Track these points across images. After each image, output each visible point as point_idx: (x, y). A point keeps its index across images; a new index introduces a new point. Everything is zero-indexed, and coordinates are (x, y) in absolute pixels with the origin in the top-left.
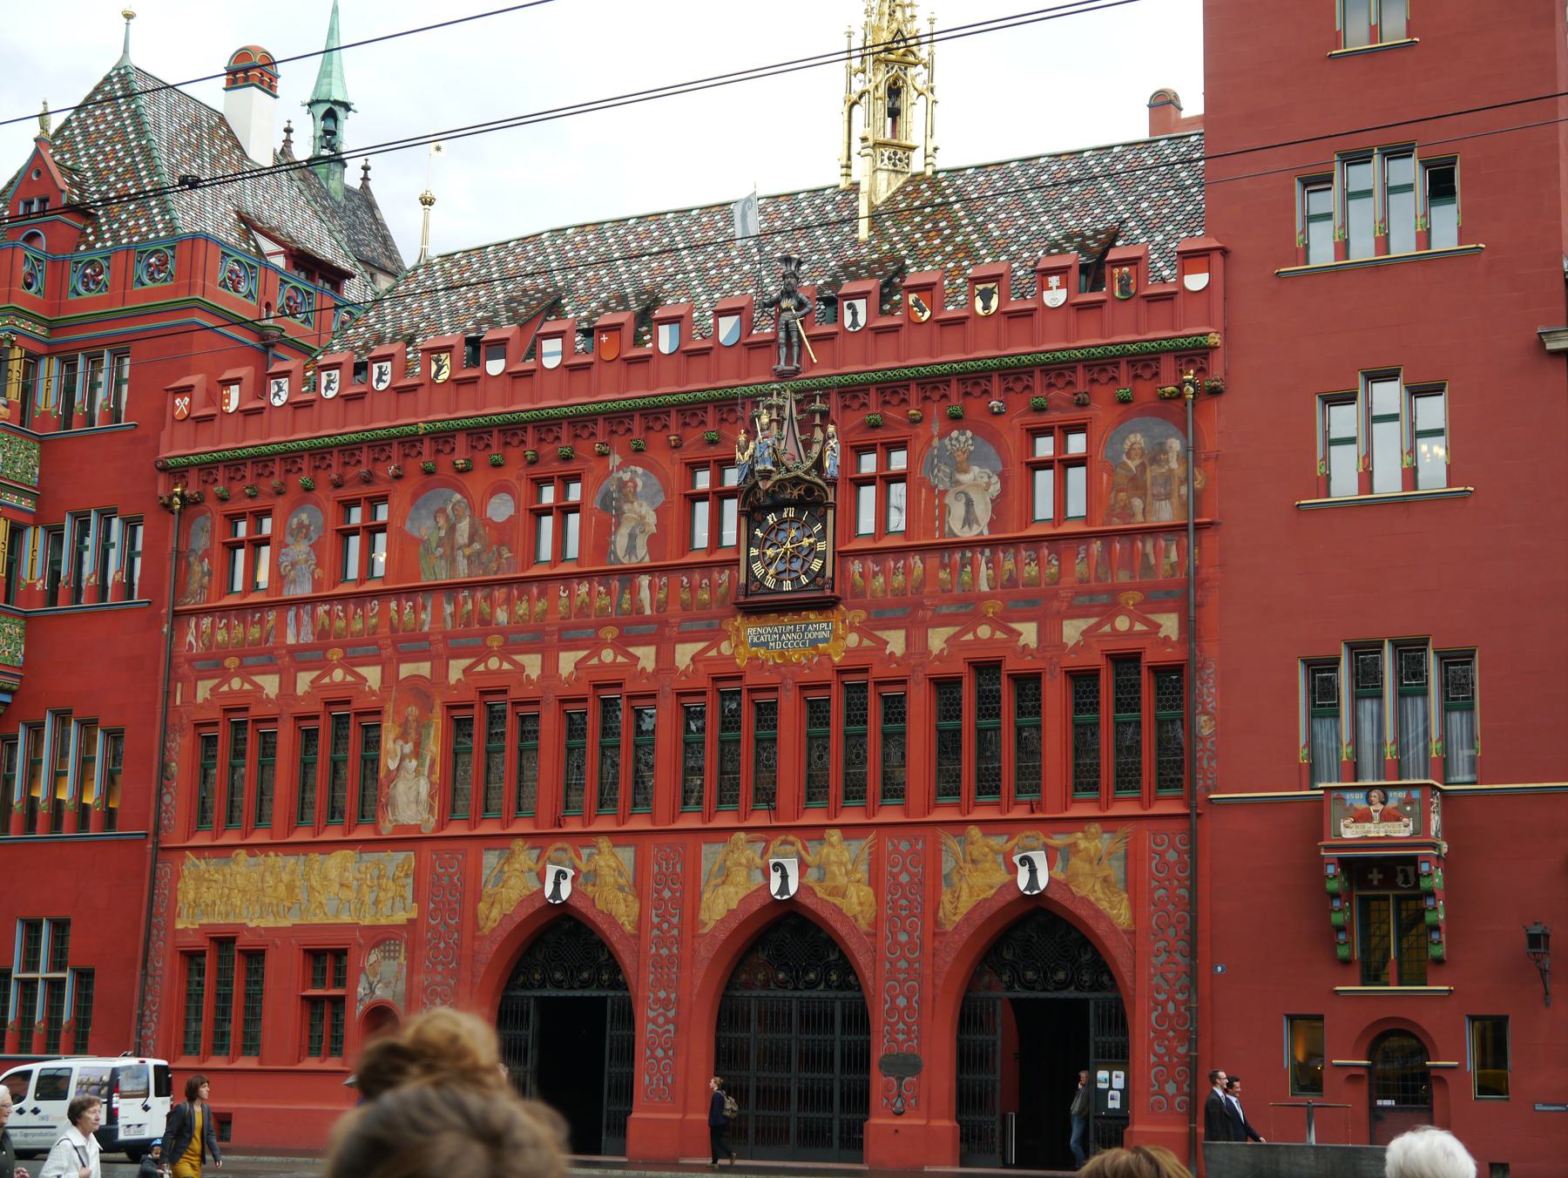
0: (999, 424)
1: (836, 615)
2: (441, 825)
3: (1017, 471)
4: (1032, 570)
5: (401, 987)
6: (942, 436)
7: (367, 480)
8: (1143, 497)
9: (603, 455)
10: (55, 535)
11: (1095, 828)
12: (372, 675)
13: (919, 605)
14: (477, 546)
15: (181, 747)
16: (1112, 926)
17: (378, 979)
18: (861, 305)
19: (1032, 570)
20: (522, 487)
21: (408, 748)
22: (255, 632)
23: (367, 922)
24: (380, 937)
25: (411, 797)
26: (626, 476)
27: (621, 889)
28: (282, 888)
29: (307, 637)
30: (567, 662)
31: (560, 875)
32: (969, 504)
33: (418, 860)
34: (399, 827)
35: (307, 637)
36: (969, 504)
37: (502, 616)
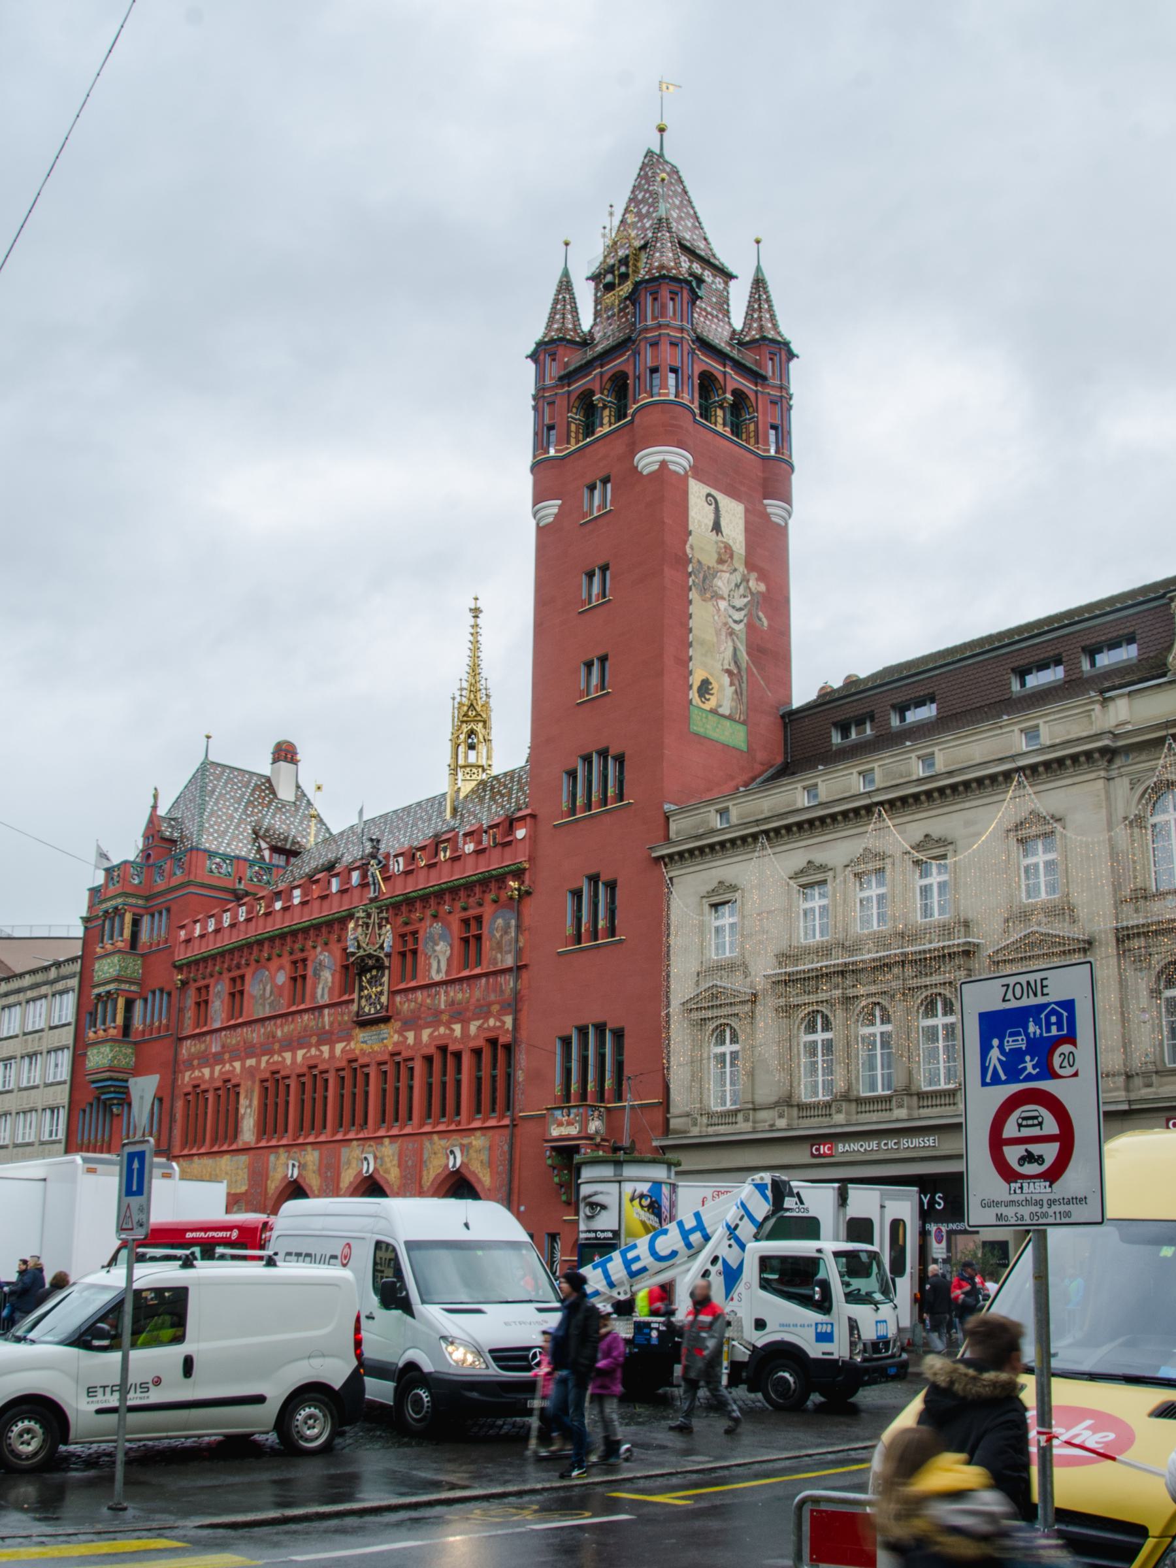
0: (451, 918)
1: (390, 1025)
2: (258, 1140)
3: (456, 942)
4: (460, 996)
6: (431, 926)
7: (238, 967)
8: (501, 953)
9: (314, 947)
10: (146, 1000)
11: (478, 1133)
12: (237, 1065)
13: (419, 1018)
15: (179, 1104)
16: (483, 1186)
18: (401, 859)
19: (460, 996)
20: (288, 966)
21: (248, 1103)
22: (203, 1047)
26: (322, 957)
30: (300, 1053)
31: (294, 1165)
32: (439, 962)
35: (219, 1049)
36: (439, 962)
37: (279, 1033)
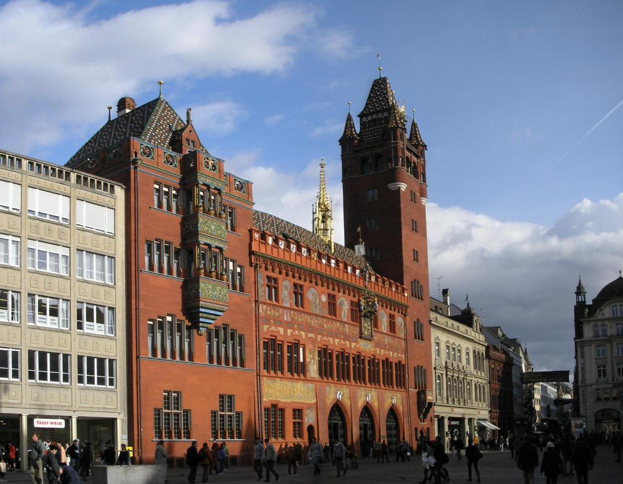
5: (315, 419)
11: (399, 392)
12: (303, 333)
14: (320, 307)
17: (309, 418)
21: (311, 356)
22: (277, 314)
23: (306, 402)
24: (309, 406)
25: (313, 369)
27: (347, 398)
28: (288, 391)
29: (289, 320)
31: (340, 394)
33: (316, 386)
34: (311, 377)
37: (325, 326)
